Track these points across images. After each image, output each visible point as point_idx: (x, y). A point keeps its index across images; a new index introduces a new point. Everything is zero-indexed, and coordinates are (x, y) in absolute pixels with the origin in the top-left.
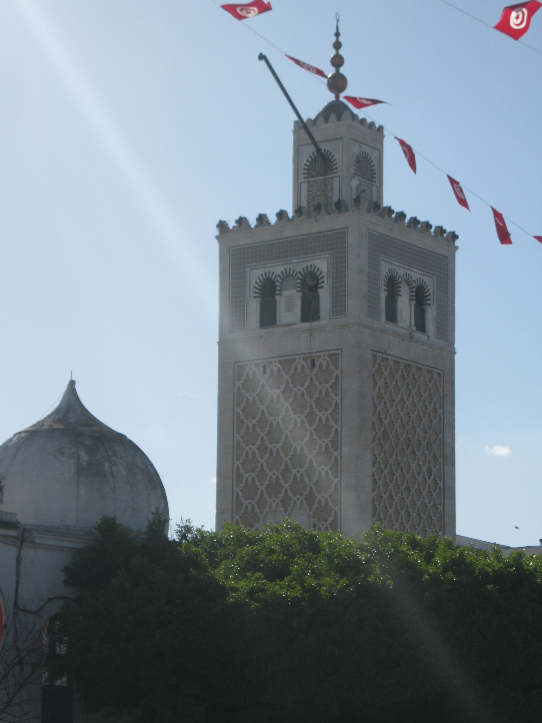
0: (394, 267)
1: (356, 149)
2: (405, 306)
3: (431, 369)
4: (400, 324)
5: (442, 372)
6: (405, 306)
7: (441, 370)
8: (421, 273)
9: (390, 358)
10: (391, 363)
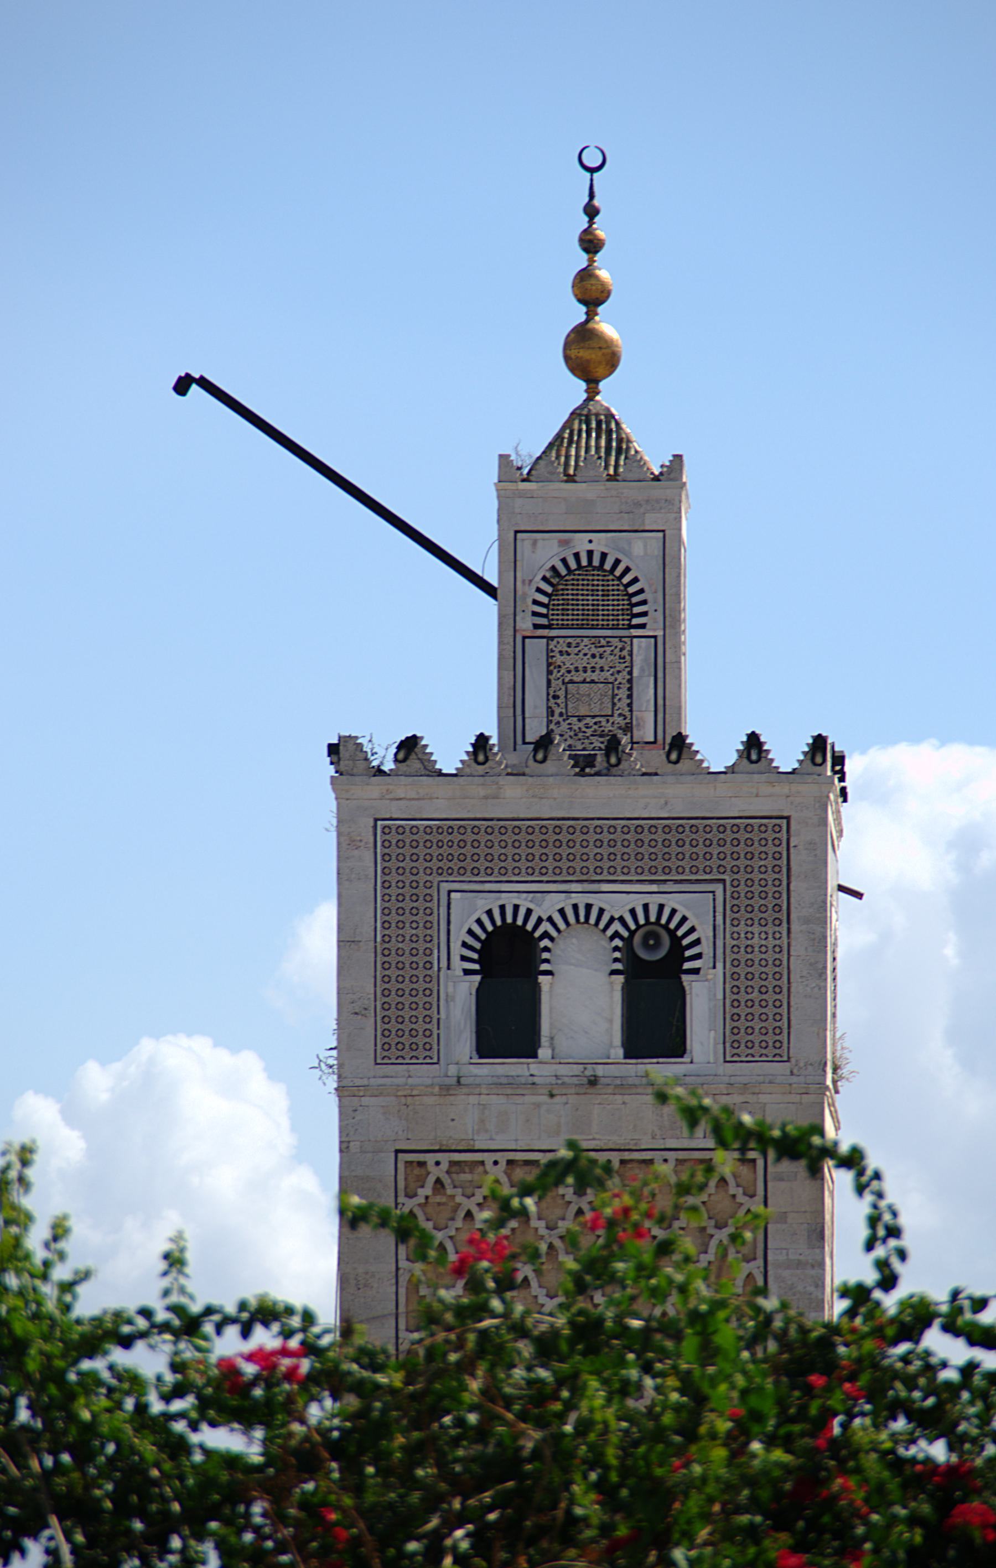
0: (509, 901)
1: (545, 555)
2: (581, 998)
6: (581, 998)
8: (654, 888)
9: (488, 1158)
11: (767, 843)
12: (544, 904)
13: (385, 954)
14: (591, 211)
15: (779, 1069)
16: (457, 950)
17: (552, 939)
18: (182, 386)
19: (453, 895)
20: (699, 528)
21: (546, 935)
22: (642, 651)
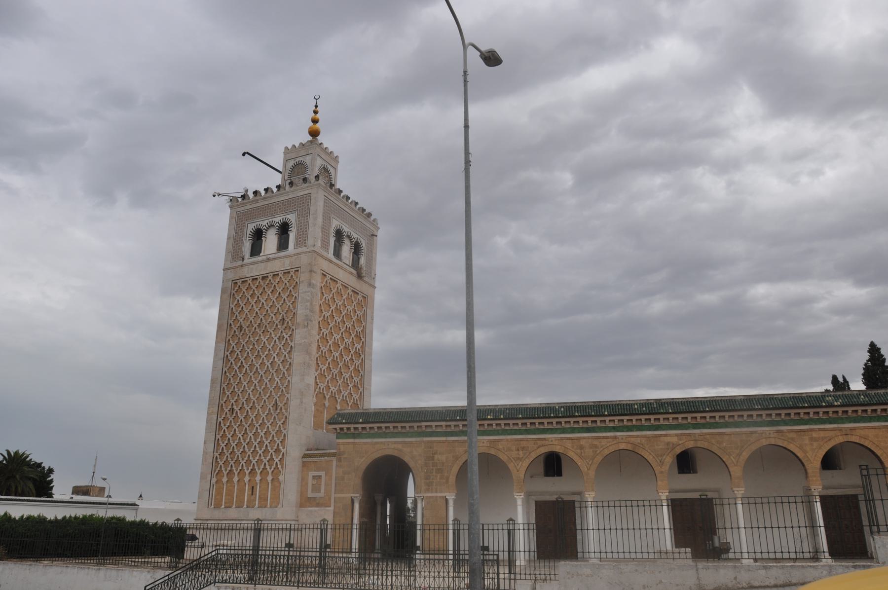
1: (291, 164)
2: (271, 242)
6: (271, 242)
14: (316, 106)
18: (244, 154)
20: (340, 167)
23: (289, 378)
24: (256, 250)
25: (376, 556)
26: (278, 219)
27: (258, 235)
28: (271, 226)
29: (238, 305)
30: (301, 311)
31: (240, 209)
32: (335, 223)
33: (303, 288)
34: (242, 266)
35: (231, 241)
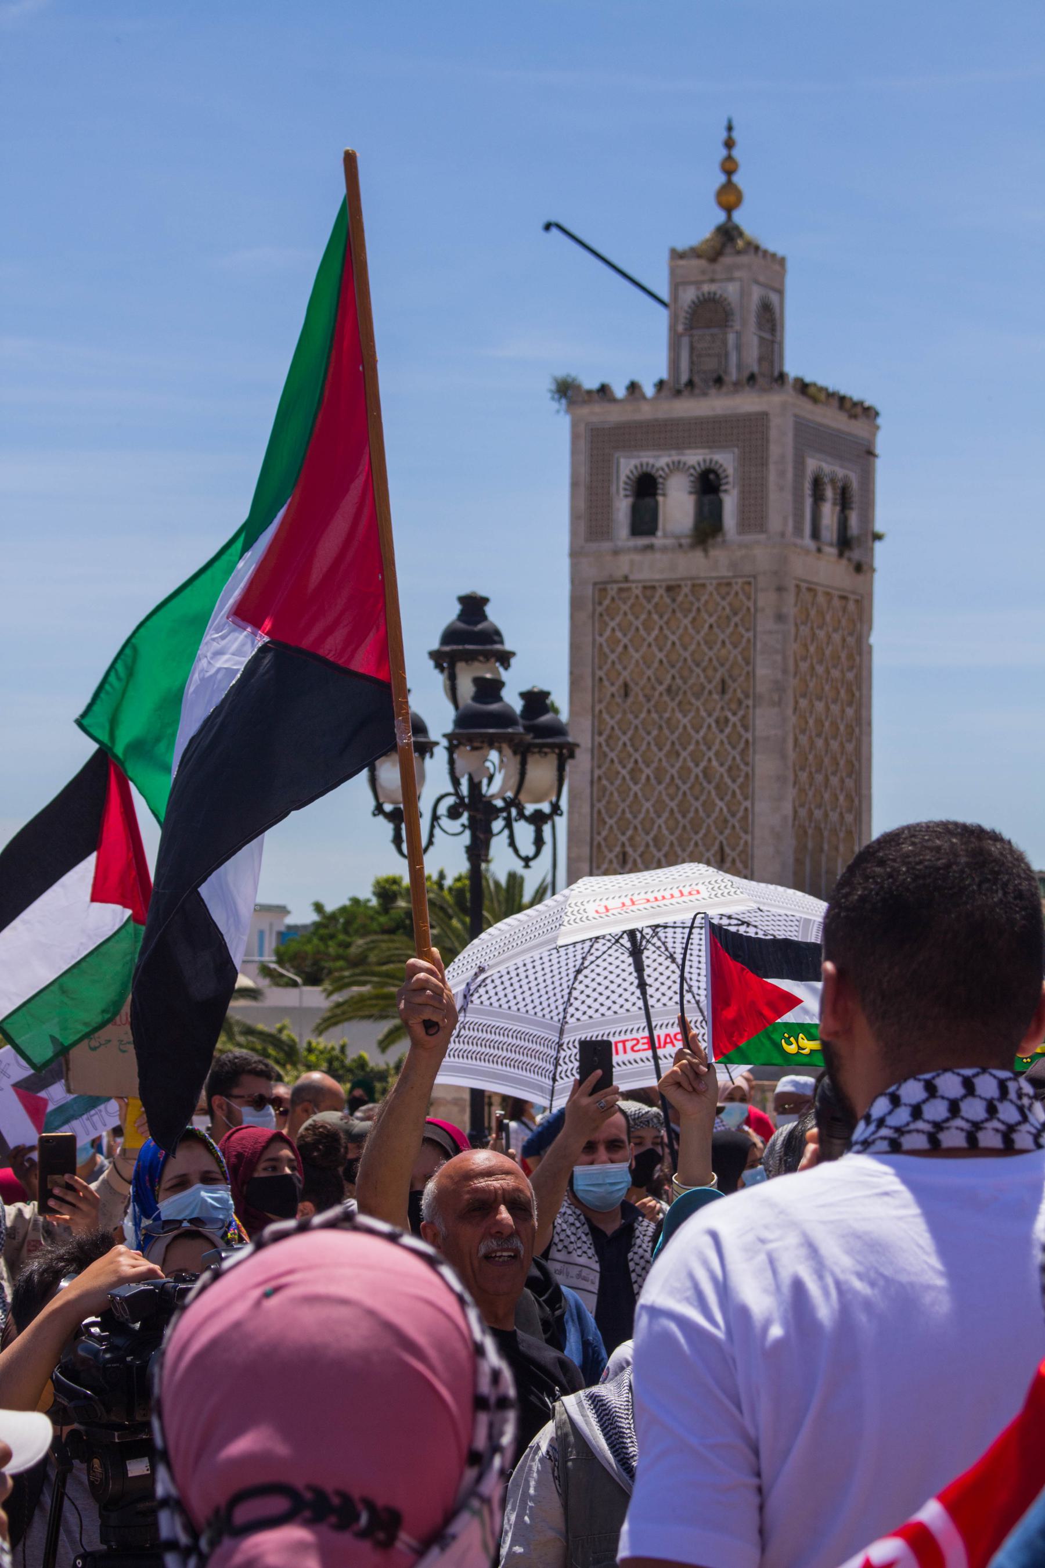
0: (644, 460)
1: (689, 295)
2: (678, 506)
3: (725, 581)
4: (659, 533)
5: (752, 580)
6: (678, 506)
7: (749, 576)
9: (634, 585)
10: (638, 591)
11: (844, 431)
12: (659, 461)
13: (591, 490)
15: (762, 537)
16: (622, 485)
17: (664, 479)
18: (548, 227)
19: (622, 460)
21: (661, 476)
22: (731, 338)
23: (748, 804)
24: (645, 521)
25: (631, 1107)
26: (695, 458)
27: (646, 487)
28: (677, 467)
29: (613, 642)
30: (764, 671)
31: (595, 419)
32: (812, 464)
33: (765, 623)
34: (616, 552)
35: (582, 490)
